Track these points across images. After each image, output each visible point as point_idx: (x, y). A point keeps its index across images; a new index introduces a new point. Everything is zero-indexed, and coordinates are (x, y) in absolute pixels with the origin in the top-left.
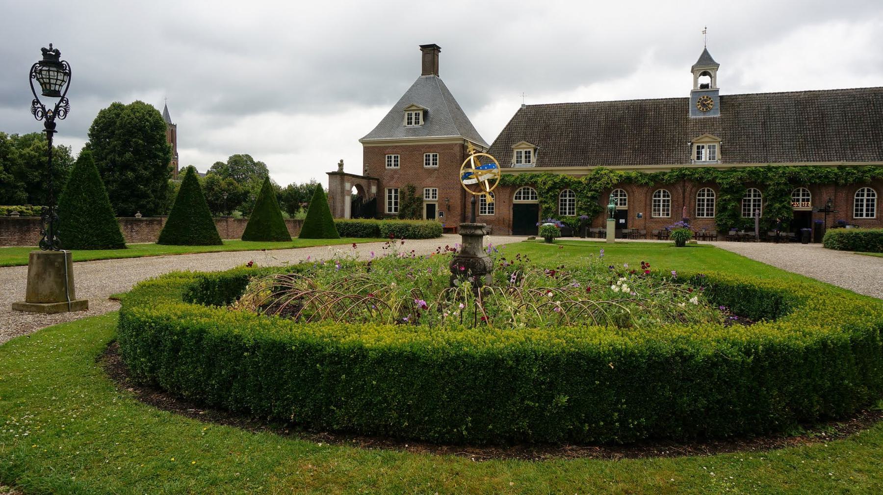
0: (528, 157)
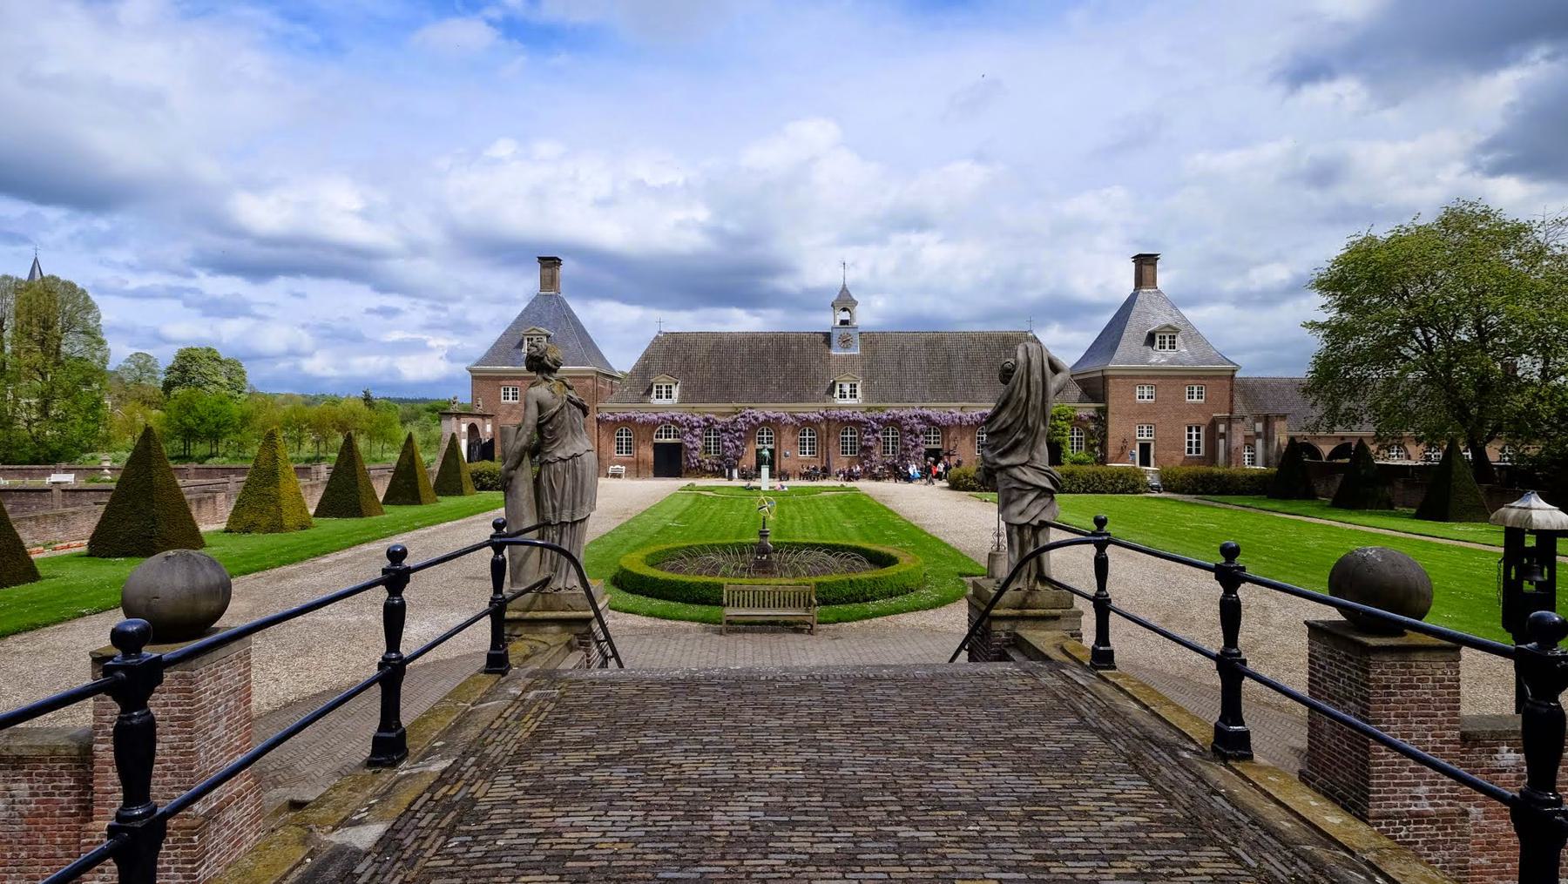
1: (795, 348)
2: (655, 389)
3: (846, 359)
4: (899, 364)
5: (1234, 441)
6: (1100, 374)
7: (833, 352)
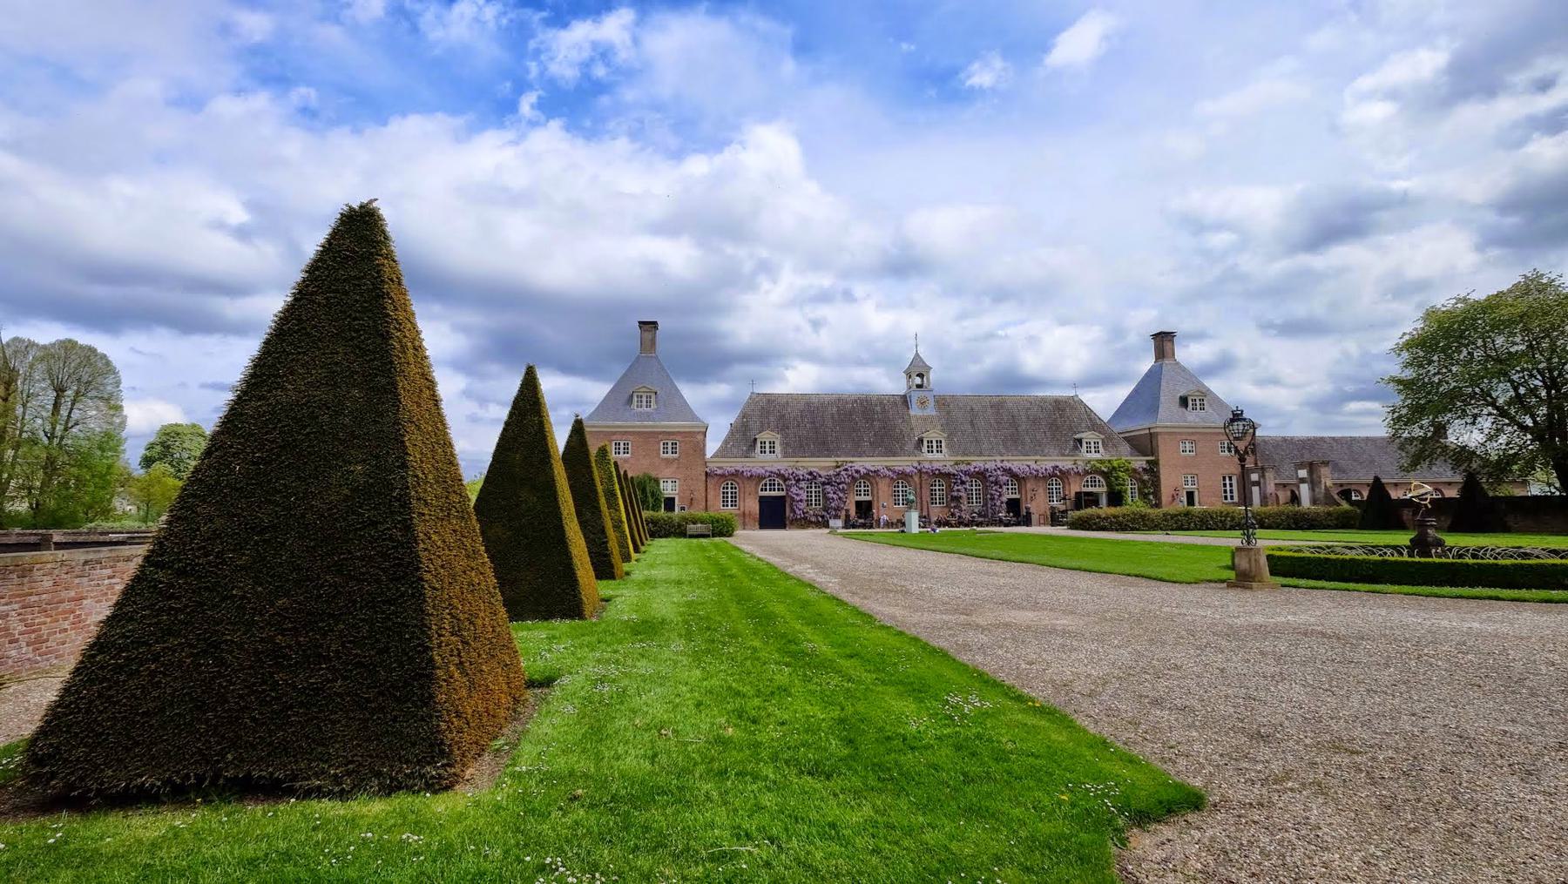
0: (772, 447)
1: (878, 408)
2: (759, 445)
3: (925, 419)
4: (972, 423)
5: (1268, 487)
6: (1147, 431)
7: (912, 413)
